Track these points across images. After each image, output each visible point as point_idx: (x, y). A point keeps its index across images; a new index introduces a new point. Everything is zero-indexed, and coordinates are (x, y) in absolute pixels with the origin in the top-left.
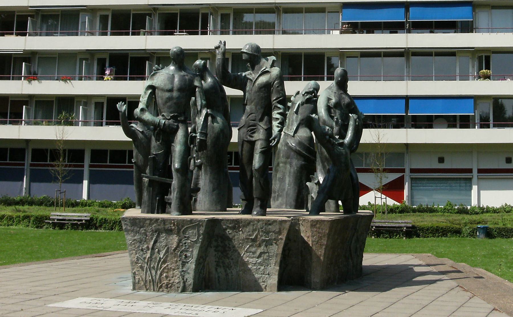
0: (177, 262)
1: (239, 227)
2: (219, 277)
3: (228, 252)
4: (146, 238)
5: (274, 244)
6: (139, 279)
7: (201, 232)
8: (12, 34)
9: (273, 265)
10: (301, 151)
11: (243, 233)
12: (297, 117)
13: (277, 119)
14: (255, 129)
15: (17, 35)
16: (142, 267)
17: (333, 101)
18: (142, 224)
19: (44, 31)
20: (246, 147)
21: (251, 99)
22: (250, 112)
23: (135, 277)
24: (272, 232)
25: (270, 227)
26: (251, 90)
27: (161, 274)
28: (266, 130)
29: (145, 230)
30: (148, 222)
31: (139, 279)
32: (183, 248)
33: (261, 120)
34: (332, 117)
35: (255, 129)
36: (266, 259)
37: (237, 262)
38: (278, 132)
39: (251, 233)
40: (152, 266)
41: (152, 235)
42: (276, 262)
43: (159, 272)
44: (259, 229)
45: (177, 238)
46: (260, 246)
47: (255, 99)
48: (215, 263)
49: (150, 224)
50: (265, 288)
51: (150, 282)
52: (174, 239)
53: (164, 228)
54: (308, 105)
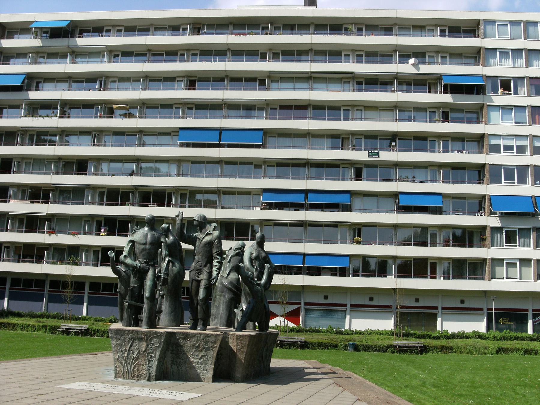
0: (145, 360)
1: (188, 338)
2: (173, 371)
3: (180, 355)
4: (124, 343)
5: (211, 350)
6: (119, 370)
7: (162, 340)
8: (39, 202)
9: (209, 365)
10: (232, 288)
11: (190, 342)
12: (229, 265)
13: (216, 266)
15: (43, 203)
16: (121, 363)
17: (254, 255)
18: (122, 333)
19: (61, 201)
20: (195, 284)
21: (199, 252)
23: (116, 369)
24: (210, 342)
25: (209, 338)
26: (199, 246)
27: (134, 368)
28: (208, 273)
30: (126, 332)
31: (119, 370)
32: (150, 351)
33: (205, 266)
34: (253, 266)
35: (201, 272)
36: (205, 360)
37: (186, 361)
38: (217, 274)
39: (196, 342)
40: (128, 362)
41: (129, 341)
42: (212, 363)
43: (133, 367)
44: (201, 340)
46: (201, 351)
47: (201, 252)
48: (171, 362)
50: (204, 380)
51: (126, 373)
52: (144, 345)
53: (137, 337)
54: (237, 257)
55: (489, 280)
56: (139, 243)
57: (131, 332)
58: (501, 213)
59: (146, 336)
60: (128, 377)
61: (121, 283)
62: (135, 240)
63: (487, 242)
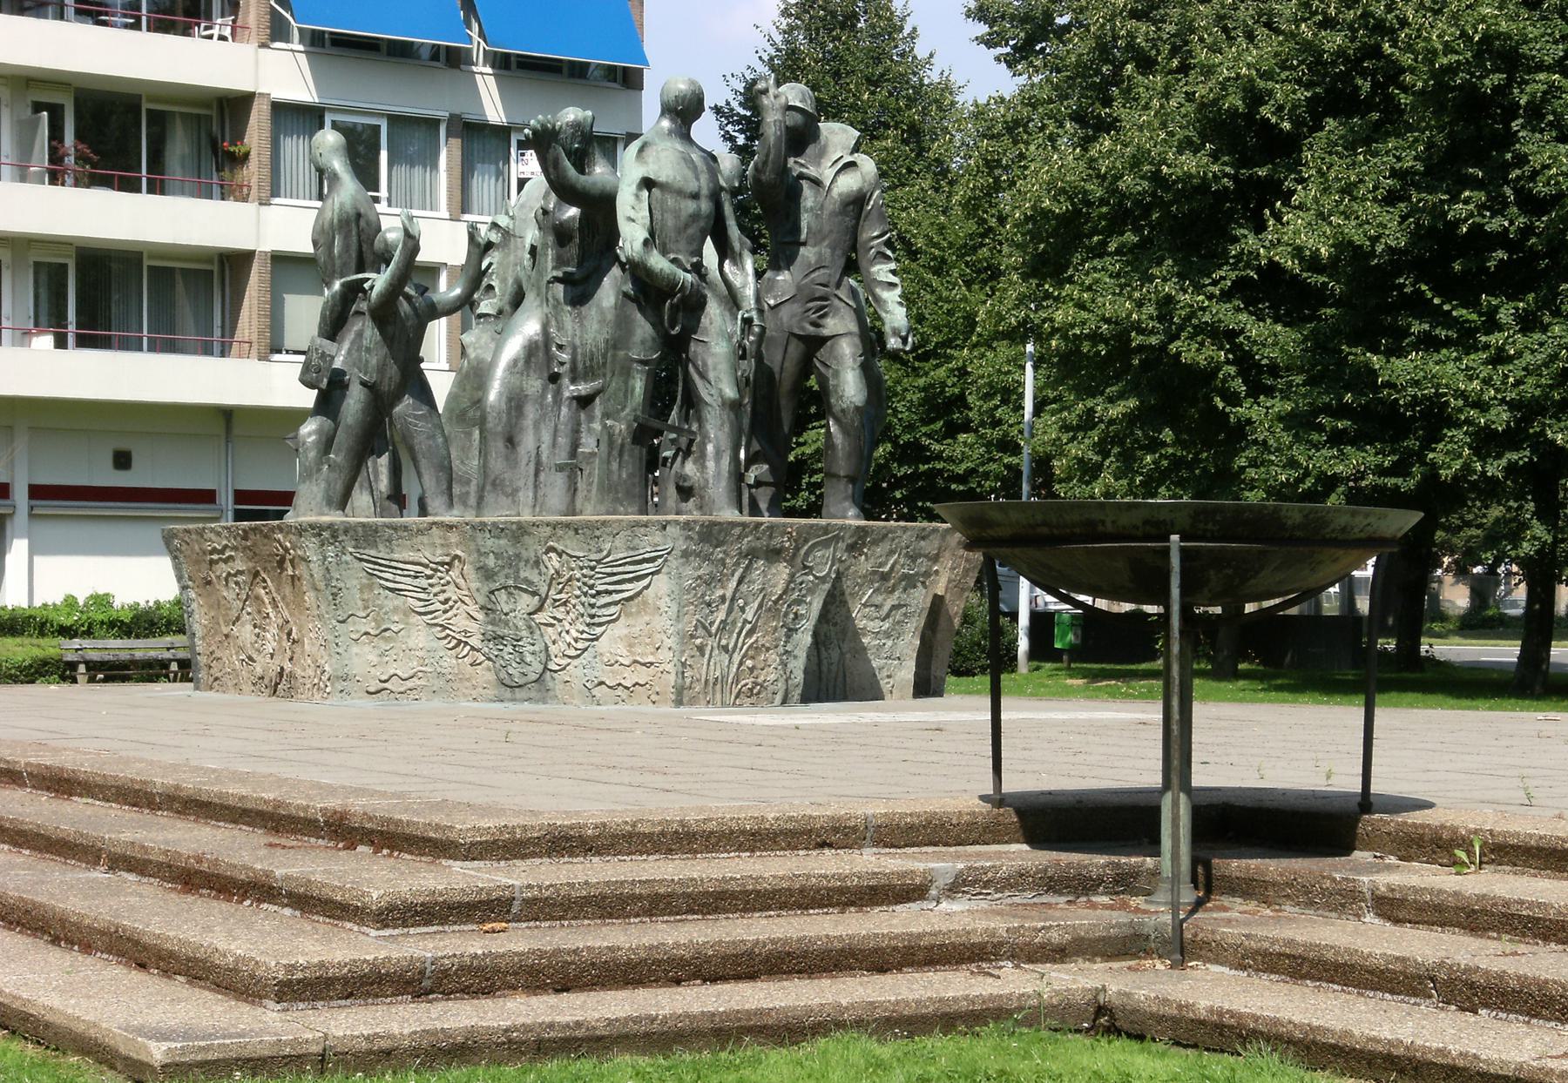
0: (775, 629)
1: (864, 545)
4: (721, 573)
5: (919, 584)
11: (867, 560)
13: (892, 285)
14: (826, 307)
20: (795, 349)
21: (820, 231)
22: (817, 262)
27: (741, 664)
29: (725, 552)
30: (737, 531)
32: (795, 596)
35: (826, 307)
36: (898, 622)
39: (883, 559)
41: (737, 564)
43: (737, 658)
45: (787, 571)
47: (831, 231)
49: (739, 537)
51: (714, 684)
52: (782, 572)
53: (768, 546)
55: (263, 358)
56: (680, 193)
57: (751, 532)
58: (308, 37)
59: (795, 541)
60: (718, 696)
61: (390, 347)
62: (662, 179)
63: (254, 172)
